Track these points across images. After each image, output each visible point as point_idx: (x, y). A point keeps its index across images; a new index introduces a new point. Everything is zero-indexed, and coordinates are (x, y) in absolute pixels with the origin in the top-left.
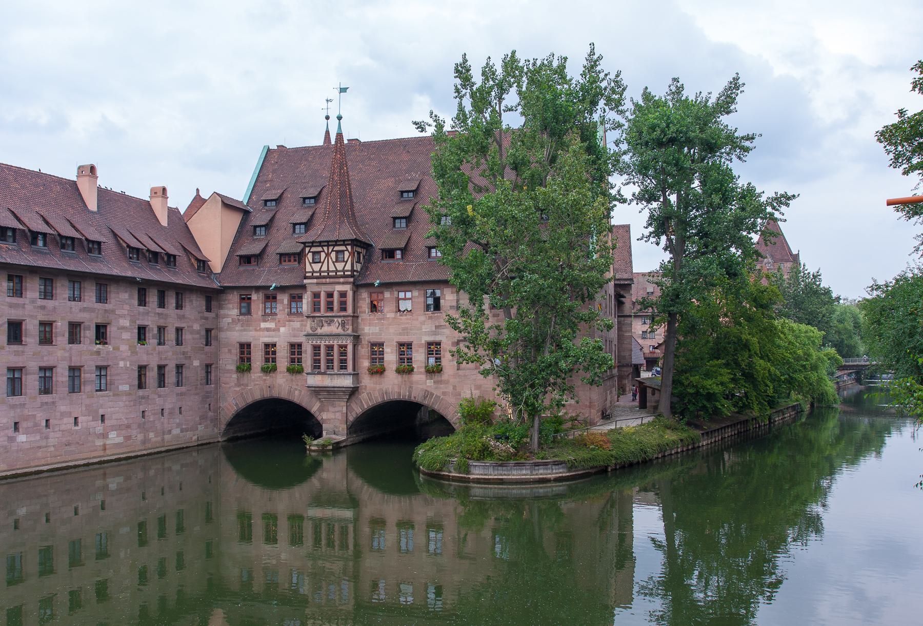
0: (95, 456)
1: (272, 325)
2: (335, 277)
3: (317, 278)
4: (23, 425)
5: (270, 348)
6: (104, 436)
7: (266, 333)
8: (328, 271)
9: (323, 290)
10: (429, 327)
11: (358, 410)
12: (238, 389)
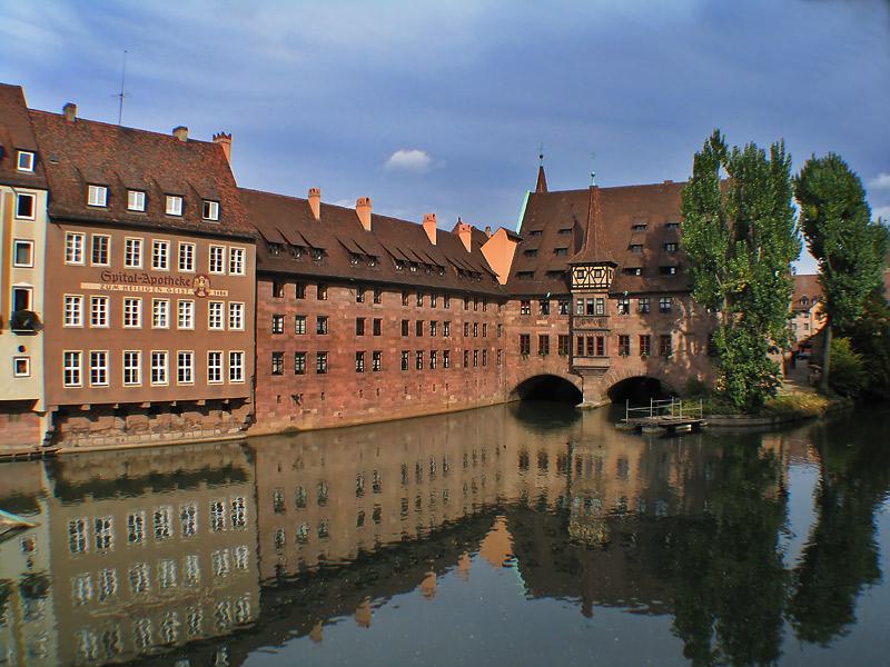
0: (445, 410)
1: (546, 322)
2: (594, 288)
4: (410, 388)
5: (544, 339)
6: (448, 398)
11: (611, 385)
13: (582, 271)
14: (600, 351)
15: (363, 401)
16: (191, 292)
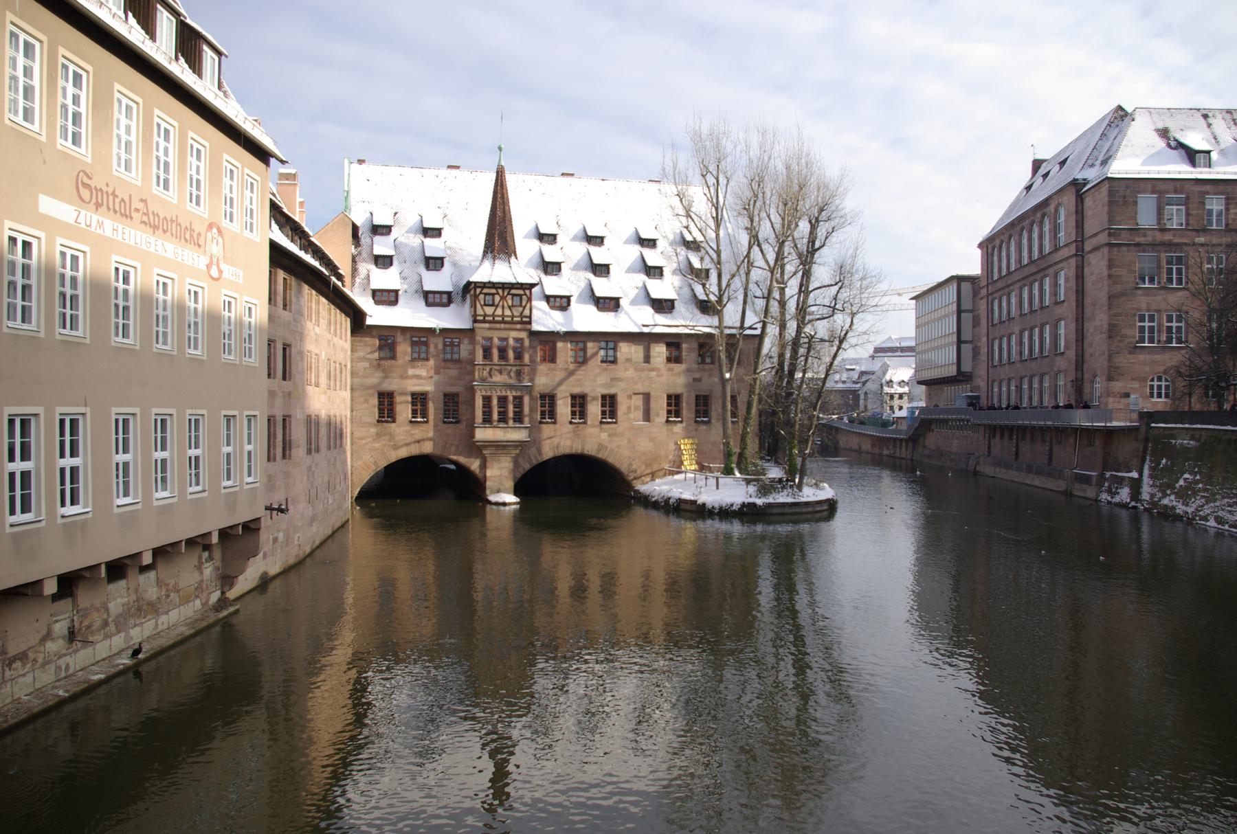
3: (489, 322)
7: (415, 381)
8: (503, 316)
9: (496, 336)
10: (603, 379)
11: (527, 467)
12: (376, 445)
13: (493, 295)
14: (519, 418)
15: (309, 512)
16: (202, 262)
